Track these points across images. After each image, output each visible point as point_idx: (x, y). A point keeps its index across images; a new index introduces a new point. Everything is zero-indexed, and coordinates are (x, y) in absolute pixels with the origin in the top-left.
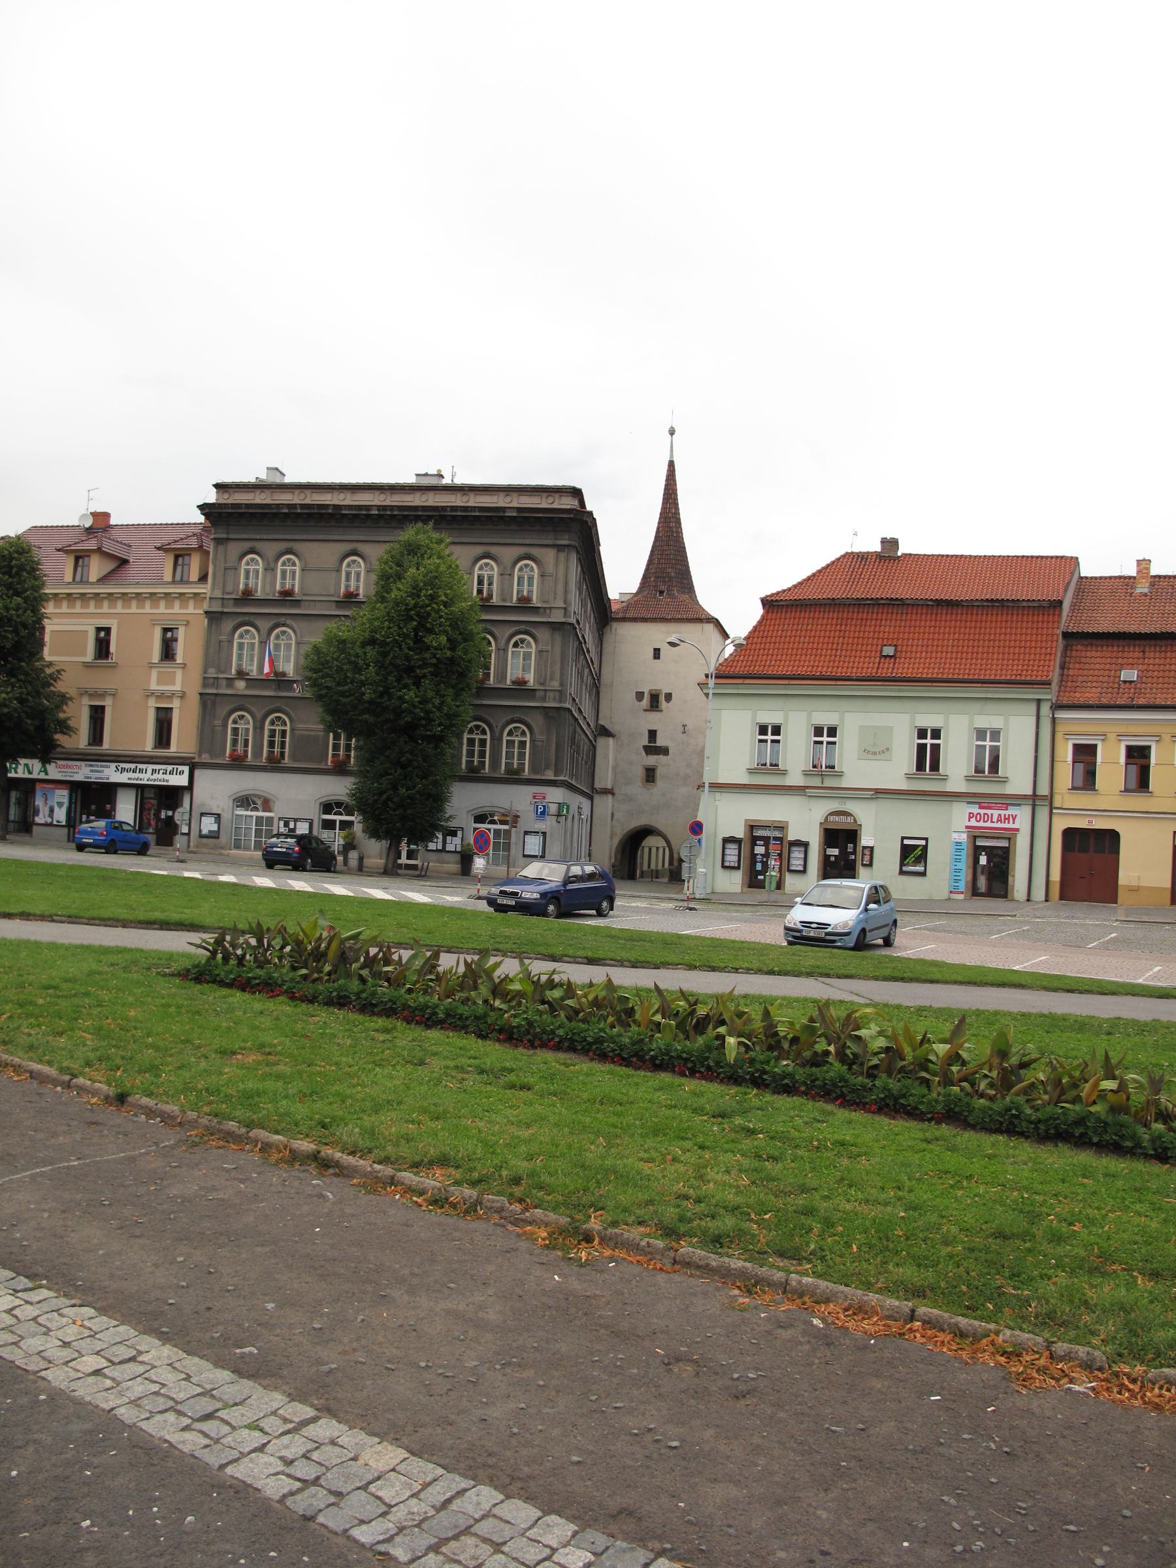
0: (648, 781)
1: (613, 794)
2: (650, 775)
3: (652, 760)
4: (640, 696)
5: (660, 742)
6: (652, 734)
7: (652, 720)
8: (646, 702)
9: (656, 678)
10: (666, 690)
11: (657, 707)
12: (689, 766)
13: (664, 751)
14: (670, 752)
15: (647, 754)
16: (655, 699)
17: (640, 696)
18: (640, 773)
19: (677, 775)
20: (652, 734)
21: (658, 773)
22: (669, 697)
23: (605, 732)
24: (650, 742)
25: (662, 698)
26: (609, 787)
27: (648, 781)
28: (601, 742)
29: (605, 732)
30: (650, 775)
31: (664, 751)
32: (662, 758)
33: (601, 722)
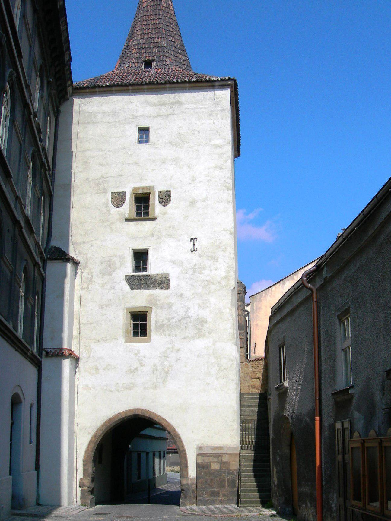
0: (135, 334)
2: (139, 323)
3: (140, 299)
4: (118, 199)
5: (154, 267)
6: (140, 258)
7: (140, 234)
8: (128, 207)
9: (148, 171)
11: (147, 214)
13: (164, 283)
14: (173, 283)
15: (132, 287)
16: (142, 203)
17: (118, 199)
18: (122, 321)
20: (140, 258)
21: (152, 321)
22: (165, 198)
24: (137, 270)
25: (155, 201)
27: (135, 334)
30: (139, 323)
31: (164, 283)
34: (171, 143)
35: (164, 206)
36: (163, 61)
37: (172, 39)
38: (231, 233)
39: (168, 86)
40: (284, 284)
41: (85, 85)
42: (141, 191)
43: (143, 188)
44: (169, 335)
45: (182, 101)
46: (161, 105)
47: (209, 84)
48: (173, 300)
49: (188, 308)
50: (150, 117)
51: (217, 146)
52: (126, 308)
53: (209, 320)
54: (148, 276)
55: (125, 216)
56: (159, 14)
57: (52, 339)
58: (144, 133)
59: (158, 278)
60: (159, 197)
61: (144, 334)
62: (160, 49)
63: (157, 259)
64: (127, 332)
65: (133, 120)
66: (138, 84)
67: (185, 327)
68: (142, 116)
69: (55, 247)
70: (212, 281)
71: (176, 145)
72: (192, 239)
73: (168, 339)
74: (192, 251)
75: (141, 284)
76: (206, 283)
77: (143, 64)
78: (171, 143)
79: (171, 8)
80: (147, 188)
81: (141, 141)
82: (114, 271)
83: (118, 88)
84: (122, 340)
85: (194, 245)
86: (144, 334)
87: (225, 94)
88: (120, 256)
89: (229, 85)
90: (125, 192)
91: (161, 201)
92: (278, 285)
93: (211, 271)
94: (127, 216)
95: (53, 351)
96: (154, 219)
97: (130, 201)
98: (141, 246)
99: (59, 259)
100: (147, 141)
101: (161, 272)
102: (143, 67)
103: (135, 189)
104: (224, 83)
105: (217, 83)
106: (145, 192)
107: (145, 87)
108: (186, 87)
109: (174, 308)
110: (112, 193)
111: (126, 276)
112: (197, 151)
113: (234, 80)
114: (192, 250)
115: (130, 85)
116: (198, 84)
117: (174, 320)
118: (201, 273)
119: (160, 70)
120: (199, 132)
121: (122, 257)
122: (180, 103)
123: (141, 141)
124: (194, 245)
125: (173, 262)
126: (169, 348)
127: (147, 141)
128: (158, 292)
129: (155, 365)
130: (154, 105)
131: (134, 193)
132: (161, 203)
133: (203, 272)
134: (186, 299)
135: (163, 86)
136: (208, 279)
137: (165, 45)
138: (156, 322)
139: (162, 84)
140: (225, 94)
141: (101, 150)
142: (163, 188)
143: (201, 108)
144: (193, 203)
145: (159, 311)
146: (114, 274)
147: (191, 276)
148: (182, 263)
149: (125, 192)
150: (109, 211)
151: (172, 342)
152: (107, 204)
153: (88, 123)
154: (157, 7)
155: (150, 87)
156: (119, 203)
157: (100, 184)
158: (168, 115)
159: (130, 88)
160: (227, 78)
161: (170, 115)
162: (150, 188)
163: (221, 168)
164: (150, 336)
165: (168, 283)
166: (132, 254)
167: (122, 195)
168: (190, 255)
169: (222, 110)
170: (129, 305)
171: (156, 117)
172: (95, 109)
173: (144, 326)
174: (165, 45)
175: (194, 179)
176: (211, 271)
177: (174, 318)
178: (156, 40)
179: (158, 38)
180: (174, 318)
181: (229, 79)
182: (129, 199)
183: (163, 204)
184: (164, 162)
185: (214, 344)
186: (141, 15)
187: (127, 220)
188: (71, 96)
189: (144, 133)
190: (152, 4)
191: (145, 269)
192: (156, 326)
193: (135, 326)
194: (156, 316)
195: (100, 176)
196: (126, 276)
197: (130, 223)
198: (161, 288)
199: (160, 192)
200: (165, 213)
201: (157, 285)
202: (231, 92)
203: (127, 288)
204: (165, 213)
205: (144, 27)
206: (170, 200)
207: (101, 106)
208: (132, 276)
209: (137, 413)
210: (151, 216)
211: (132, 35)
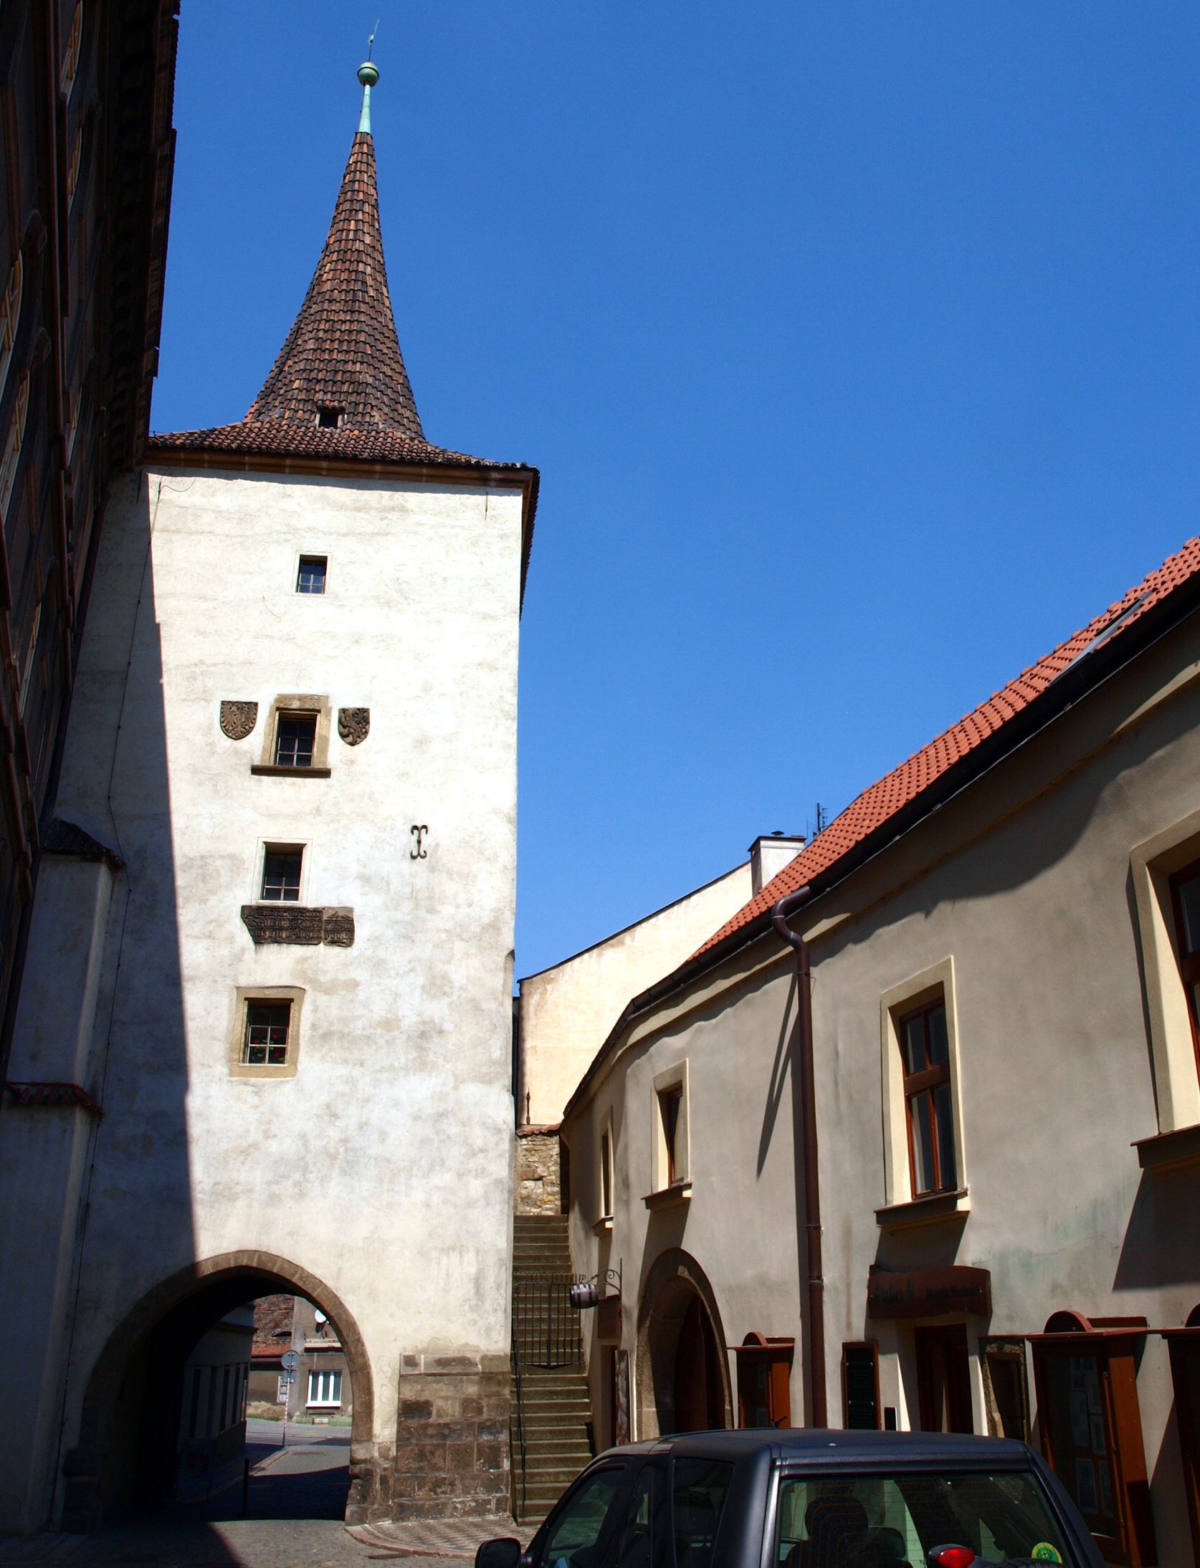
1: (96, 1114)
2: (268, 1025)
3: (277, 966)
4: (237, 718)
6: (283, 863)
7: (285, 808)
8: (260, 741)
10: (342, 698)
11: (307, 760)
12: (437, 985)
13: (337, 928)
14: (361, 931)
15: (258, 940)
17: (237, 718)
19: (389, 1024)
20: (283, 863)
21: (304, 1021)
22: (355, 724)
23: (83, 847)
24: (268, 894)
25: (328, 728)
26: (79, 1077)
27: (256, 1057)
28: (56, 879)
29: (83, 847)
31: (337, 928)
32: (324, 956)
33: (66, 812)
34: (378, 598)
35: (352, 744)
36: (363, 415)
37: (385, 369)
38: (510, 822)
39: (378, 468)
40: (600, 955)
41: (178, 442)
42: (296, 705)
43: (301, 698)
44: (345, 1061)
45: (409, 506)
46: (359, 510)
47: (475, 474)
48: (360, 974)
49: (397, 996)
50: (331, 534)
51: (486, 617)
52: (238, 988)
53: (448, 1026)
54: (302, 911)
55: (252, 760)
56: (360, 312)
57: (34, 1058)
58: (313, 569)
59: (325, 917)
60: (340, 722)
61: (278, 1056)
62: (359, 387)
63: (326, 870)
64: (232, 1050)
65: (287, 536)
66: (307, 456)
67: (387, 1041)
68: (310, 529)
69: (62, 822)
70: (458, 931)
71: (389, 604)
72: (415, 828)
73: (342, 1070)
74: (413, 857)
75: (281, 929)
76: (444, 936)
77: (318, 416)
78: (378, 598)
79: (387, 304)
80: (311, 697)
81: (302, 588)
82: (213, 892)
83: (257, 460)
84: (221, 1069)
85: (419, 842)
86: (278, 1056)
87: (510, 506)
88: (232, 857)
89: (521, 482)
90: (256, 704)
91: (345, 731)
92: (586, 955)
93: (458, 906)
94: (257, 762)
95: (33, 1091)
96: (325, 774)
97: (268, 725)
98: (285, 835)
99: (72, 853)
100: (319, 589)
101: (335, 904)
102: (317, 421)
103: (282, 698)
104: (511, 476)
105: (495, 475)
106: (307, 706)
107: (324, 464)
108: (422, 476)
109: (362, 994)
110: (223, 703)
111: (243, 908)
112: (439, 622)
113: (535, 472)
114: (415, 854)
115: (289, 454)
116: (448, 473)
117: (360, 1024)
118: (431, 910)
119: (356, 432)
120: (445, 579)
121: (236, 862)
122: (403, 509)
123: (302, 588)
124: (419, 842)
125: (365, 879)
126: (343, 1095)
127: (319, 589)
128: (323, 953)
129: (303, 1137)
130: (342, 507)
131: (278, 709)
132: (343, 736)
133: (439, 908)
134: (393, 972)
135: (366, 467)
136: (448, 925)
137: (370, 380)
138: (314, 1027)
139: (365, 461)
140: (510, 506)
141: (204, 598)
142: (354, 703)
143: (454, 527)
144: (421, 743)
145: (323, 999)
146: (213, 900)
147: (408, 918)
148: (388, 884)
149: (256, 704)
150: (212, 745)
151: (352, 1081)
152: (210, 728)
153: (177, 532)
154: (354, 295)
155: (336, 465)
156: (240, 728)
157: (195, 679)
158: (373, 534)
159: (288, 462)
160: (518, 466)
161: (379, 534)
162: (318, 698)
163: (492, 668)
164: (295, 1063)
165: (350, 931)
166: (262, 853)
167: (249, 709)
168: (408, 866)
169: (501, 537)
170: (244, 981)
171: (345, 535)
172: (197, 500)
173: (281, 1037)
174: (370, 380)
175: (427, 688)
176: (458, 906)
177: (356, 1018)
178: (350, 367)
179: (354, 363)
180: (356, 1018)
181: (524, 467)
182: (265, 724)
183: (350, 739)
184: (357, 642)
185: (456, 1088)
186: (315, 308)
187: (256, 771)
188: (140, 463)
189: (313, 569)
190: (344, 287)
191: (294, 895)
192: (312, 1037)
193: (256, 1035)
194: (315, 1010)
195: (196, 660)
196: (243, 908)
197: (265, 779)
198: (333, 943)
199: (344, 711)
200: (352, 762)
201: (322, 935)
202: (524, 498)
203: (245, 937)
204: (352, 762)
205: (321, 334)
206: (367, 732)
207: (213, 495)
208: (260, 909)
209: (245, 1262)
210: (316, 764)
211: (291, 349)
